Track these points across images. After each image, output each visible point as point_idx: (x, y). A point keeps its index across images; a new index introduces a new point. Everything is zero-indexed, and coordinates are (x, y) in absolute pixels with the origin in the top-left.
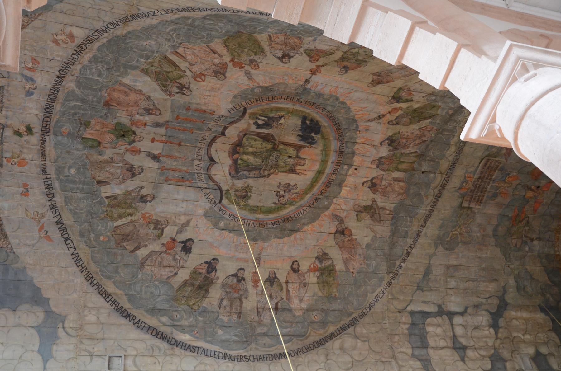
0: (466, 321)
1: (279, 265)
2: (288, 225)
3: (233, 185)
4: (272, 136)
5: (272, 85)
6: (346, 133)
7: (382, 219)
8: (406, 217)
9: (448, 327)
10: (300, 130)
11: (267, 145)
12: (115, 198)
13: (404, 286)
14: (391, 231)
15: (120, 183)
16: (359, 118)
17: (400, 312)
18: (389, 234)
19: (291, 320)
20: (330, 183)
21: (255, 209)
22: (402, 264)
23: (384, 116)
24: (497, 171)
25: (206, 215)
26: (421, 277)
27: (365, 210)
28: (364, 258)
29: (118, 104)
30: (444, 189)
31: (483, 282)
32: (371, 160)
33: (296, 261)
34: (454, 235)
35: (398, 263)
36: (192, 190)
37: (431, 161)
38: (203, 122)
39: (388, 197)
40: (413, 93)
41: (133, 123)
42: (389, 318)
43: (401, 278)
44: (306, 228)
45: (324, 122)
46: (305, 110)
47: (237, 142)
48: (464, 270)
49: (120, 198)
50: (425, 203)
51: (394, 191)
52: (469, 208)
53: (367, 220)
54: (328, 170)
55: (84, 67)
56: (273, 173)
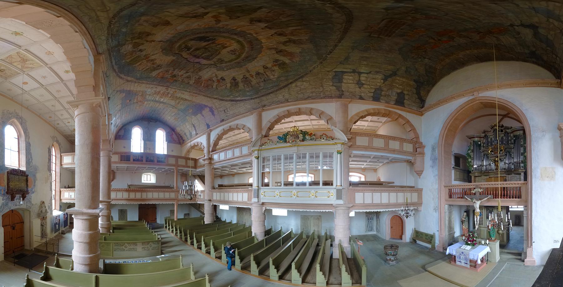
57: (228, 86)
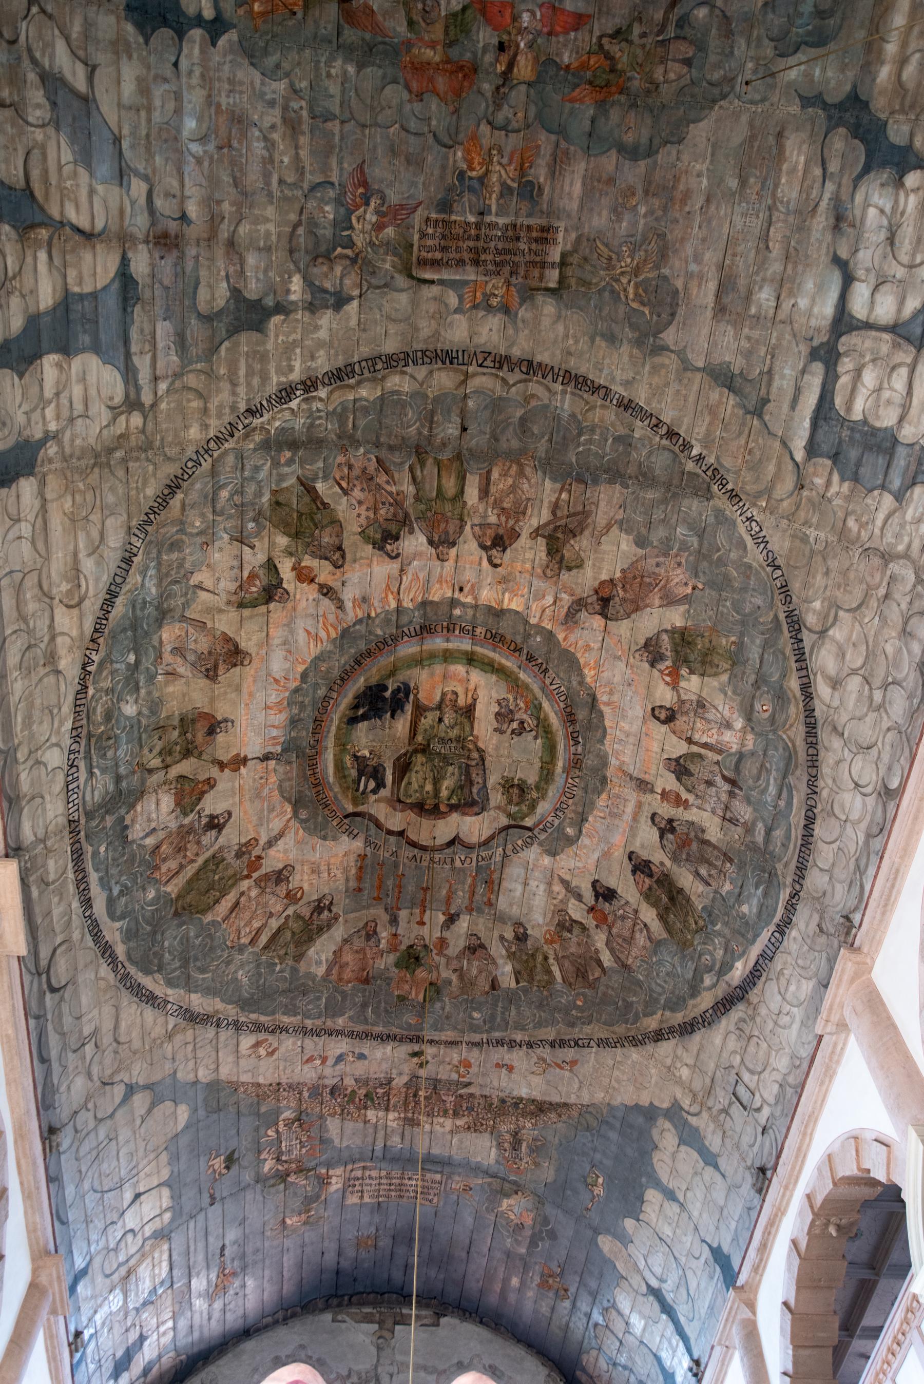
0: (868, 270)
1: (656, 747)
2: (581, 714)
3: (498, 808)
4: (398, 759)
5: (289, 800)
6: (377, 636)
7: (580, 508)
8: (579, 445)
9: (868, 344)
10: (380, 718)
11: (419, 763)
12: (519, 973)
13: (747, 457)
14: (611, 481)
15: (495, 963)
16: (335, 629)
17: (802, 487)
18: (618, 486)
19: (758, 765)
20: (493, 637)
21: (545, 772)
22: (695, 452)
23: (322, 586)
24: (453, 218)
25: (553, 854)
26: (732, 400)
27: (557, 551)
28: (666, 555)
29: (364, 970)
30: (507, 358)
31: (776, 186)
32: (438, 563)
33: (653, 709)
34: (636, 294)
35: (690, 466)
36: (507, 871)
37: (432, 422)
38: (382, 865)
39: (528, 499)
40: (246, 574)
41: (393, 948)
42: (806, 523)
43: (727, 462)
44: (589, 680)
45: (359, 683)
46: (333, 728)
47: (415, 810)
48: (734, 255)
49: (518, 967)
50: (546, 401)
51: (513, 489)
52: (563, 264)
53: (583, 543)
54: (466, 645)
55: (306, 1016)
56: (475, 744)
57: (648, 920)
